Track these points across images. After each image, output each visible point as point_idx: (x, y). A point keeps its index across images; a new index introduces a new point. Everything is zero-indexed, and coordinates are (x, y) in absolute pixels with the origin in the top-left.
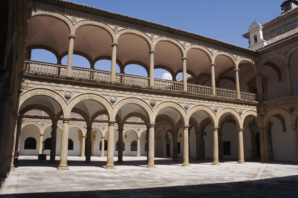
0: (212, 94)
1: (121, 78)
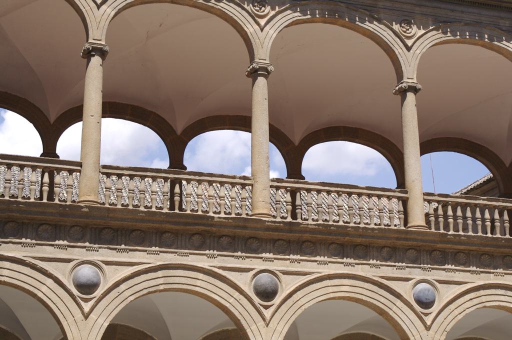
1: (52, 178)
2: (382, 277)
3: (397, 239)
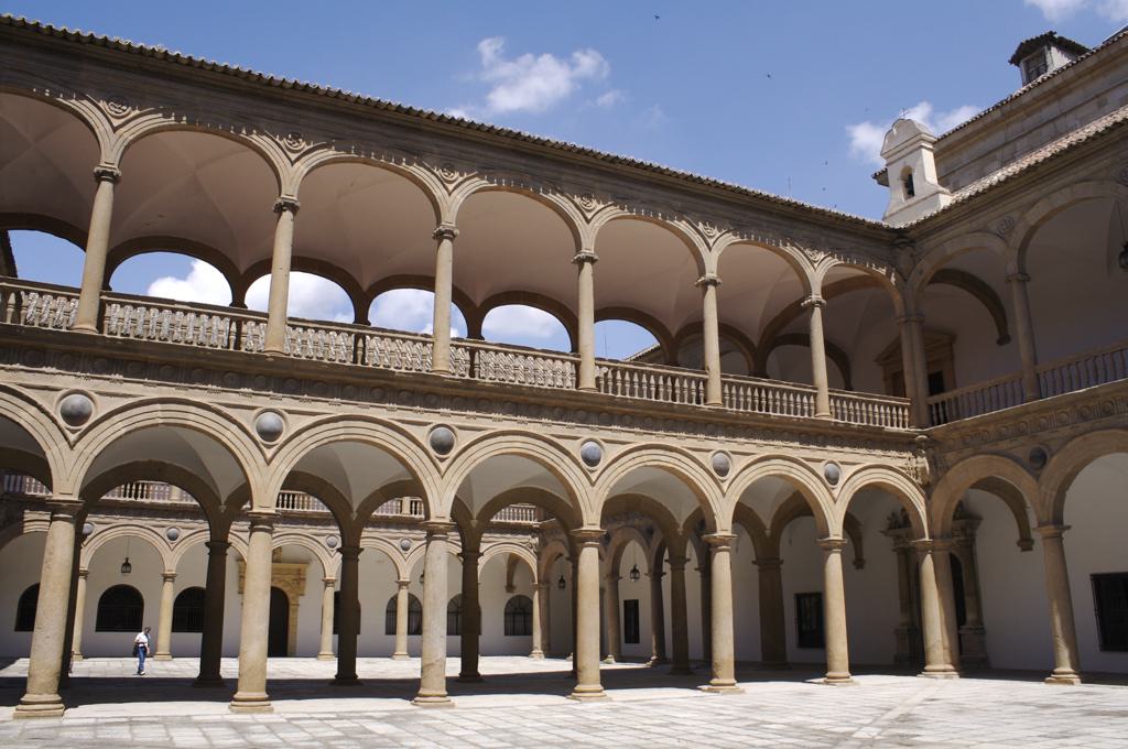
0: (705, 400)
1: (239, 327)
2: (553, 435)
3: (569, 400)
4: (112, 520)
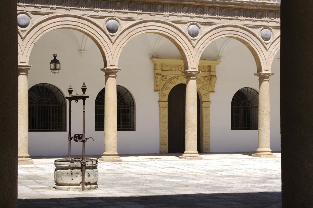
4: (49, 10)
